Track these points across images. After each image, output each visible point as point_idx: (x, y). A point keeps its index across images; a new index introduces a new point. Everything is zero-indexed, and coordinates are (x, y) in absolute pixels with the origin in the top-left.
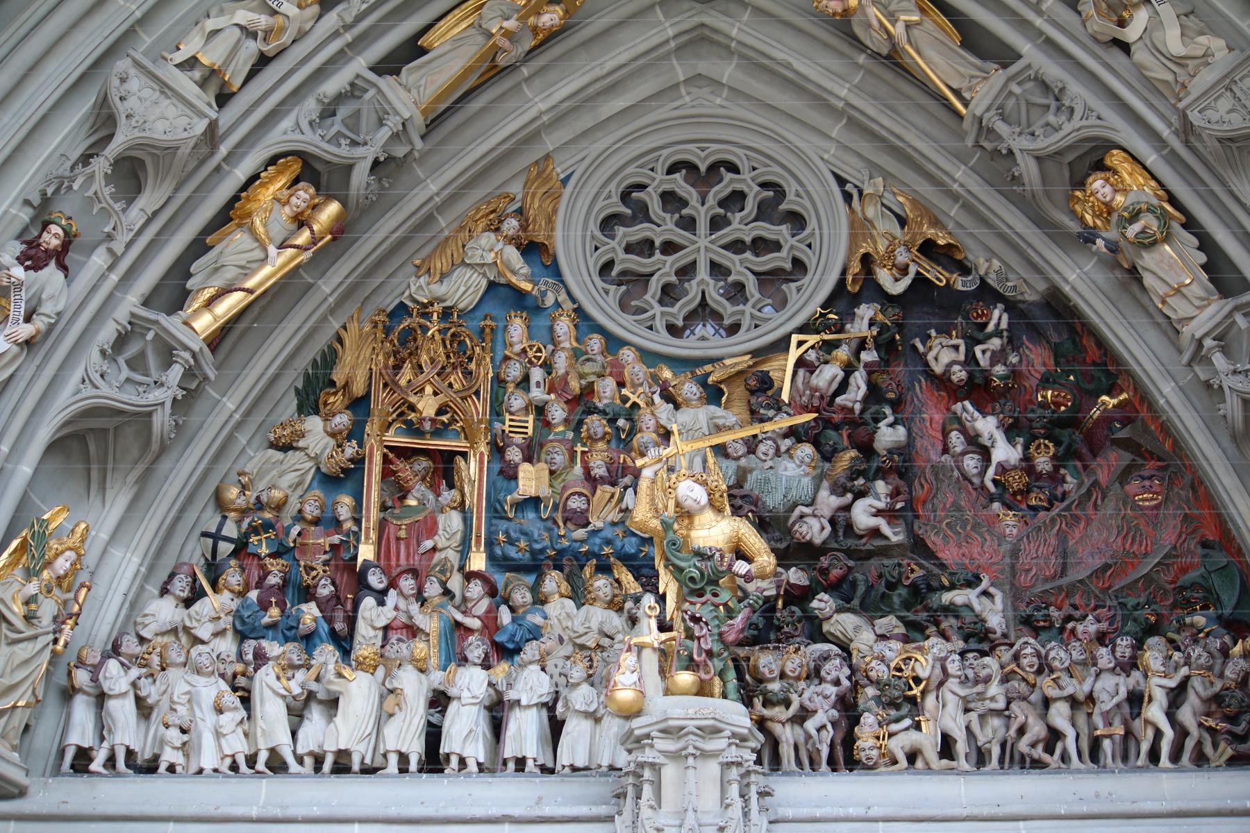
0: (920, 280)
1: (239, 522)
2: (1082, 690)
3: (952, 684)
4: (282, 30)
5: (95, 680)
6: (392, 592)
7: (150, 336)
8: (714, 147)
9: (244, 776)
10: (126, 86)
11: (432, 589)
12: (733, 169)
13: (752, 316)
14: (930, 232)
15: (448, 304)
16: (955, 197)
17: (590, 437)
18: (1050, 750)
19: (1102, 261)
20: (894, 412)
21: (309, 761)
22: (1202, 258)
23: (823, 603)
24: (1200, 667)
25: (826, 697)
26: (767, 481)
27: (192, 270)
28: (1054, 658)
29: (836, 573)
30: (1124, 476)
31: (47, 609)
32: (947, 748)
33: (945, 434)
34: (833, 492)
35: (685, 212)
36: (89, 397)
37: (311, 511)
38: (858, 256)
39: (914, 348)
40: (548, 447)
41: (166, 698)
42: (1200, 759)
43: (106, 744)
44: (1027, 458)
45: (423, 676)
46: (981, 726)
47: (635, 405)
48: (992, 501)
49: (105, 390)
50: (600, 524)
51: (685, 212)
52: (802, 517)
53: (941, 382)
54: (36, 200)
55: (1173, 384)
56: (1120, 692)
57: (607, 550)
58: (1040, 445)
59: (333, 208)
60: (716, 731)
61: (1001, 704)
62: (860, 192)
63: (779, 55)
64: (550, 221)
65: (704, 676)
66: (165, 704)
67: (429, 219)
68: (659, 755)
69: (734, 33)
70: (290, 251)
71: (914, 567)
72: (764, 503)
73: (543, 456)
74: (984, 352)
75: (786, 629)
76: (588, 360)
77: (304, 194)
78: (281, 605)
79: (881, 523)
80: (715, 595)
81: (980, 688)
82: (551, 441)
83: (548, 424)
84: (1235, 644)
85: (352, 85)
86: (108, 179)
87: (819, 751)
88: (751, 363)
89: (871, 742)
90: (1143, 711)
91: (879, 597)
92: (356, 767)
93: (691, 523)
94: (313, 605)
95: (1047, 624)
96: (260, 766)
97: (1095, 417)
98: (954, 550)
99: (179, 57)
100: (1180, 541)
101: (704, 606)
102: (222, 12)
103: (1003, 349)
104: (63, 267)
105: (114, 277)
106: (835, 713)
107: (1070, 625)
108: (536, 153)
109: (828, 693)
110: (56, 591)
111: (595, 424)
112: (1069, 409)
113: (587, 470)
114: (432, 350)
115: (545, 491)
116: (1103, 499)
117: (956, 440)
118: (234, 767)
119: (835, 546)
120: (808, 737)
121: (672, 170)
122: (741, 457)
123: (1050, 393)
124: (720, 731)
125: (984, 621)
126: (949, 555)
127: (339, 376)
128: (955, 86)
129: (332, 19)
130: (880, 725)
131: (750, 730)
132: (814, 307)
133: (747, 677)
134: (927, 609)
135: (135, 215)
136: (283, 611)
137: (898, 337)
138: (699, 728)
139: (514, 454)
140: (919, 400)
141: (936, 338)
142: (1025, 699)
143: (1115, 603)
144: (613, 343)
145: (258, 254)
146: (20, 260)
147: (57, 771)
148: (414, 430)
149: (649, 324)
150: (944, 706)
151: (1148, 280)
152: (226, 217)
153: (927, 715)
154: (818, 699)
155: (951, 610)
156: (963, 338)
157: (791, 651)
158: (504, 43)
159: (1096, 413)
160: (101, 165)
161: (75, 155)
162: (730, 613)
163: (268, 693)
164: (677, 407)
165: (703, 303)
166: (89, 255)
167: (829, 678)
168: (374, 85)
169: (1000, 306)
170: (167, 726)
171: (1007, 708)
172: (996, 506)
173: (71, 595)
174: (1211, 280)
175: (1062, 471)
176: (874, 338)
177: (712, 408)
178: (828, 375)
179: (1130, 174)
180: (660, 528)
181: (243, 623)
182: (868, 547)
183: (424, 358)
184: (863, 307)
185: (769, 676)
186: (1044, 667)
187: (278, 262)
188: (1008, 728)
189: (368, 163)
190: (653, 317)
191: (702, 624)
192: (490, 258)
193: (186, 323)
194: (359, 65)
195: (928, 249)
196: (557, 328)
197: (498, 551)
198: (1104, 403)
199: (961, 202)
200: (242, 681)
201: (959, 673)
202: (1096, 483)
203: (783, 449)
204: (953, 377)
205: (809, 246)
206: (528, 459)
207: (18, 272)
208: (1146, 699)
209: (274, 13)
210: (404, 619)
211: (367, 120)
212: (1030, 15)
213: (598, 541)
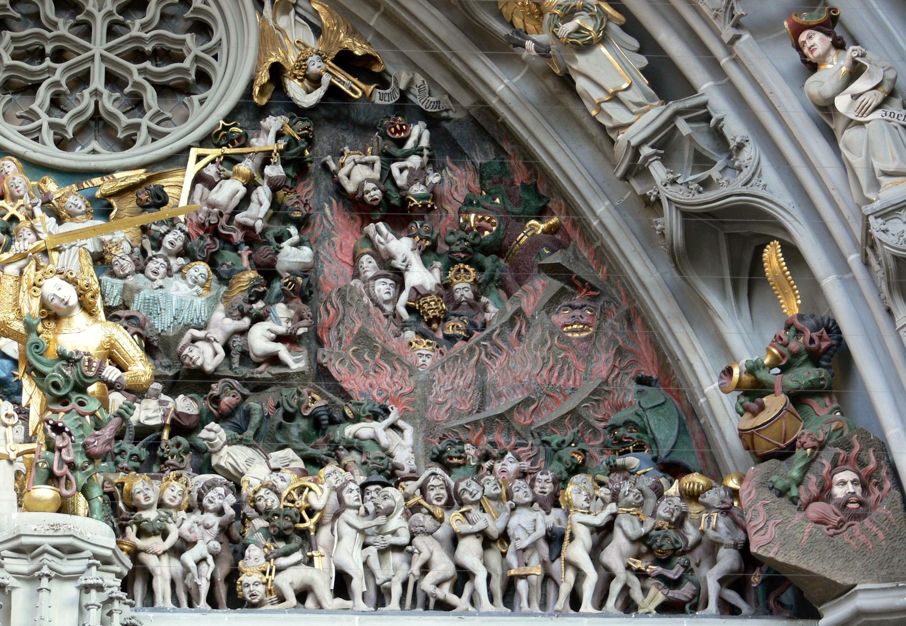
0: (333, 90)
2: (495, 529)
3: (349, 515)
14: (348, 42)
18: (458, 590)
19: (533, 73)
20: (300, 232)
22: (643, 61)
24: (629, 505)
25: (207, 527)
26: (156, 302)
28: (464, 490)
29: (227, 401)
30: (552, 304)
33: (356, 258)
34: (229, 315)
35: (80, 17)
38: (268, 65)
39: (325, 166)
42: (629, 606)
44: (446, 286)
46: (381, 563)
47: (14, 219)
48: (404, 326)
51: (80, 17)
52: (194, 340)
55: (607, 203)
56: (538, 528)
58: (459, 270)
60: (72, 551)
61: (403, 539)
65: (65, 492)
68: (8, 575)
71: (315, 396)
72: (152, 325)
74: (401, 170)
75: (170, 461)
79: (282, 350)
80: (82, 404)
81: (381, 520)
84: (671, 483)
87: (197, 586)
88: (144, 177)
89: (257, 577)
90: (563, 551)
91: (275, 428)
95: (460, 461)
97: (521, 242)
98: (360, 379)
100: (613, 376)
101: (68, 415)
106: (216, 545)
107: (486, 465)
109: (210, 523)
112: (494, 234)
116: (528, 328)
117: (369, 265)
120: (187, 570)
122: (128, 275)
123: (473, 216)
124: (78, 551)
125: (391, 456)
130: (268, 559)
131: (114, 551)
132: (216, 119)
133: (121, 504)
137: (307, 153)
138: (56, 547)
140: (329, 222)
141: (349, 154)
143: (538, 441)
149: (35, 136)
150: (339, 539)
151: (581, 84)
153: (322, 550)
154: (198, 530)
156: (379, 155)
157: (171, 478)
159: (523, 238)
162: (98, 425)
165: (96, 117)
167: (211, 507)
171: (410, 544)
172: (410, 335)
174: (652, 85)
175: (484, 299)
176: (280, 151)
180: (23, 331)
185: (144, 503)
188: (410, 563)
191: (65, 434)
195: (345, 60)
198: (532, 228)
199: (382, 9)
201: (357, 503)
202: (519, 312)
203: (175, 268)
204: (367, 196)
208: (567, 537)
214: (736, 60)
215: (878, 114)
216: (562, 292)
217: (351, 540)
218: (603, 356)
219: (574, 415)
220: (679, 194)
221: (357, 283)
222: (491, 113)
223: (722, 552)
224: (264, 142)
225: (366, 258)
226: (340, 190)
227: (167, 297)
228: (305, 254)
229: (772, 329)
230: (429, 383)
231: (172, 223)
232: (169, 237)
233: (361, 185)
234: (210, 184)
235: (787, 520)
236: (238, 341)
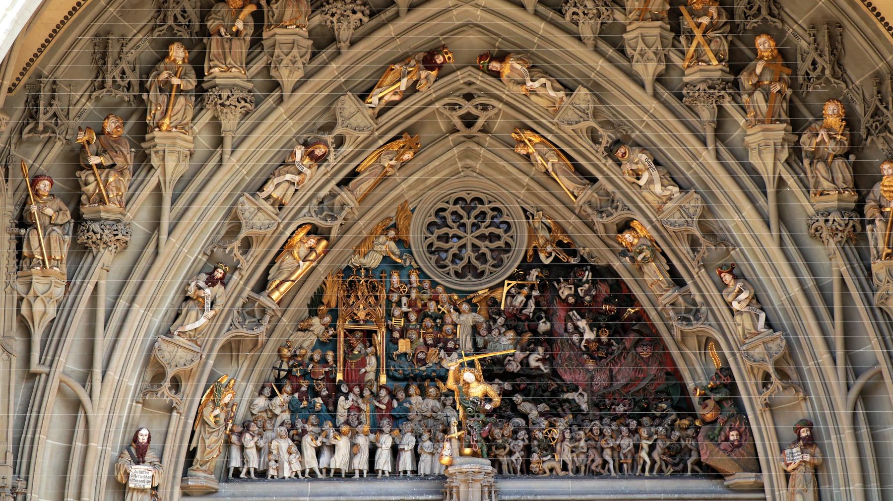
0: (556, 259)
1: (288, 362)
3: (566, 443)
4: (304, 179)
5: (240, 440)
6: (351, 394)
9: (300, 480)
11: (367, 393)
14: (561, 237)
15: (367, 266)
16: (571, 224)
18: (603, 467)
21: (324, 471)
23: (518, 398)
26: (496, 347)
29: (522, 386)
30: (636, 344)
31: (223, 416)
32: (565, 467)
33: (566, 325)
35: (462, 221)
37: (317, 357)
40: (410, 332)
43: (245, 467)
44: (598, 335)
45: (367, 438)
47: (443, 312)
48: (584, 354)
50: (431, 365)
51: (462, 221)
54: (209, 253)
57: (434, 374)
59: (324, 243)
61: (585, 450)
64: (407, 230)
67: (361, 232)
69: (482, 152)
70: (308, 263)
76: (424, 293)
78: (307, 400)
81: (577, 444)
82: (411, 329)
86: (239, 248)
89: (536, 465)
92: (343, 476)
93: (469, 386)
94: (320, 398)
96: (307, 475)
102: (279, 175)
105: (242, 283)
107: (613, 407)
108: (402, 201)
110: (225, 409)
111: (428, 322)
112: (615, 314)
113: (425, 341)
114: (362, 289)
115: (409, 351)
118: (297, 476)
119: (522, 372)
120: (512, 462)
121: (456, 202)
124: (480, 472)
125: (580, 406)
126: (567, 378)
127: (325, 301)
128: (571, 190)
129: (323, 168)
132: (514, 269)
134: (558, 400)
139: (396, 335)
142: (595, 448)
144: (434, 284)
147: (227, 480)
148: (356, 322)
155: (567, 400)
159: (625, 315)
160: (237, 244)
163: (308, 446)
164: (460, 313)
165: (469, 262)
169: (589, 267)
172: (585, 356)
177: (474, 314)
178: (521, 298)
179: (641, 230)
181: (293, 407)
182: (535, 374)
183: (360, 294)
184: (534, 270)
186: (602, 434)
187: (304, 266)
193: (269, 296)
195: (560, 244)
200: (296, 438)
202: (625, 349)
203: (502, 332)
206: (402, 336)
207: (208, 291)
209: (300, 173)
212: (602, 166)
213: (430, 371)
214: (699, 276)
217: (567, 449)
219: (644, 389)
221: (566, 334)
222: (615, 271)
223: (693, 453)
228: (548, 326)
230: (592, 378)
232: (499, 320)
233: (568, 296)
234: (513, 296)
236: (525, 361)
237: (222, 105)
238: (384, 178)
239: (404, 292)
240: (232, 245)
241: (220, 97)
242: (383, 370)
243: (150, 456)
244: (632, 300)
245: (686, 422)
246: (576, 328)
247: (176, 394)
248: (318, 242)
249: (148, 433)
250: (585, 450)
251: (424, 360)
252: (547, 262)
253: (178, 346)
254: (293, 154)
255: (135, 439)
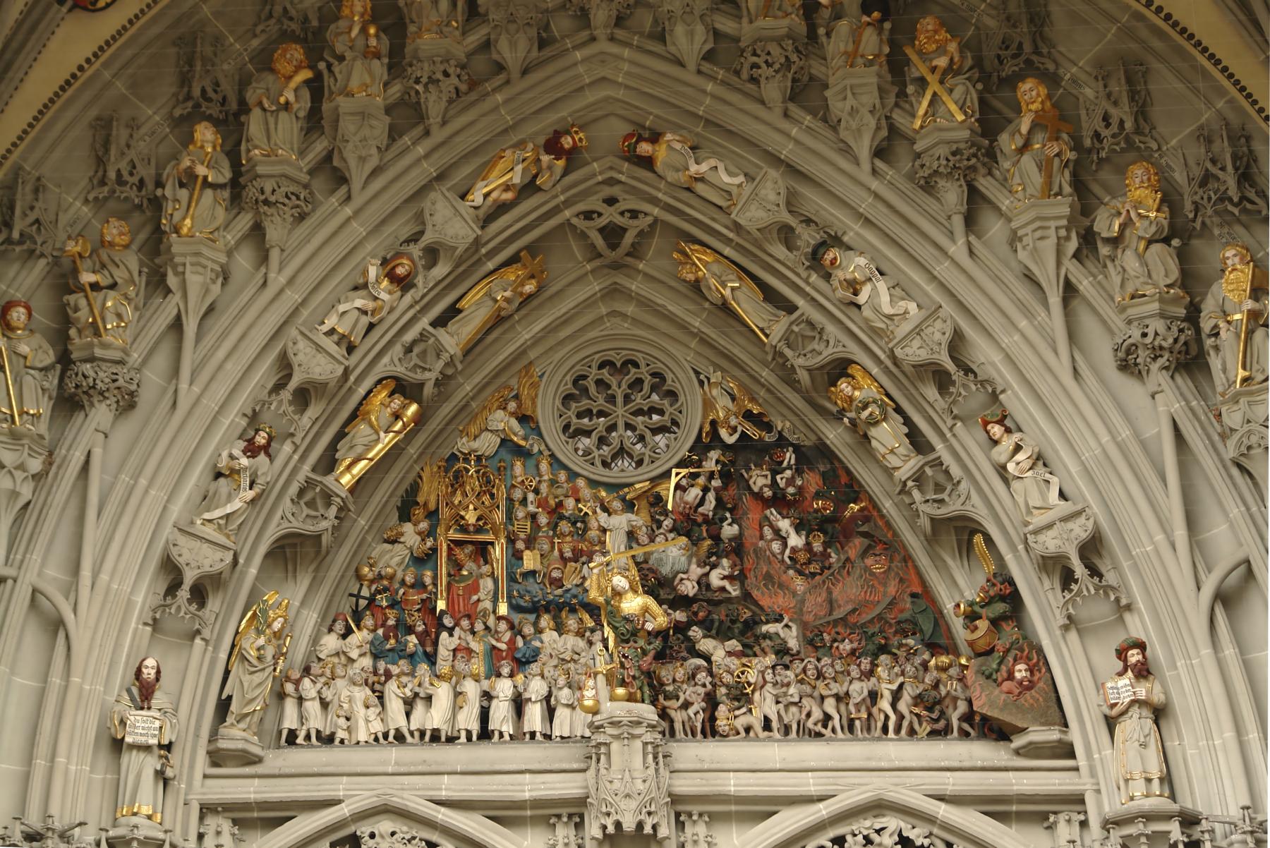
6: (457, 629)
7: (318, 490)
8: (624, 352)
10: (296, 347)
11: (479, 626)
12: (636, 365)
13: (650, 456)
14: (750, 406)
17: (562, 534)
27: (338, 447)
30: (865, 553)
31: (269, 652)
33: (761, 528)
35: (609, 392)
36: (286, 528)
39: (742, 475)
40: (539, 541)
41: (336, 697)
43: (304, 727)
48: (788, 568)
49: (295, 524)
50: (569, 586)
51: (609, 392)
53: (758, 496)
57: (574, 601)
59: (413, 408)
62: (709, 379)
63: (660, 302)
66: (336, 701)
69: (634, 287)
70: (391, 435)
73: (537, 546)
77: (397, 402)
83: (539, 527)
85: (421, 334)
86: (291, 403)
99: (325, 328)
103: (793, 477)
104: (269, 455)
105: (296, 457)
111: (565, 526)
112: (832, 512)
115: (538, 567)
117: (768, 532)
118: (376, 739)
119: (701, 597)
121: (601, 366)
129: (408, 298)
132: (684, 452)
135: (306, 420)
136: (397, 641)
139: (520, 545)
144: (573, 475)
145: (374, 437)
146: (244, 452)
147: (279, 747)
152: (354, 416)
158: (504, 305)
159: (847, 514)
160: (286, 395)
161: (270, 385)
163: (393, 696)
164: (610, 515)
165: (622, 448)
166: (282, 445)
168: (434, 336)
169: (791, 449)
170: (338, 716)
172: (791, 572)
173: (282, 642)
175: (829, 550)
177: (630, 515)
178: (694, 494)
187: (387, 440)
189: (433, 382)
190: (594, 458)
192: (501, 426)
194: (424, 323)
195: (748, 415)
196: (541, 467)
197: (514, 602)
198: (852, 508)
200: (377, 687)
202: (848, 559)
205: (680, 412)
206: (527, 548)
207: (244, 461)
210: (464, 644)
211: (431, 356)
215: (1031, 472)
216: (869, 547)
218: (893, 583)
220: (928, 509)
221: (761, 544)
224: (710, 465)
225: (766, 528)
226: (749, 486)
227: (667, 556)
229: (981, 580)
231: (665, 513)
232: (666, 523)
233: (761, 488)
234: (684, 490)
235: (991, 693)
236: (704, 579)
237: (266, 202)
238: (499, 320)
239: (531, 486)
240: (279, 398)
241: (262, 192)
242: (503, 597)
243: (159, 699)
244: (854, 490)
245: (944, 659)
246: (777, 531)
247: (197, 610)
248: (405, 407)
249: (155, 664)
250: (797, 699)
251: (560, 580)
252: (731, 440)
253: (201, 538)
254: (365, 272)
255: (139, 672)
